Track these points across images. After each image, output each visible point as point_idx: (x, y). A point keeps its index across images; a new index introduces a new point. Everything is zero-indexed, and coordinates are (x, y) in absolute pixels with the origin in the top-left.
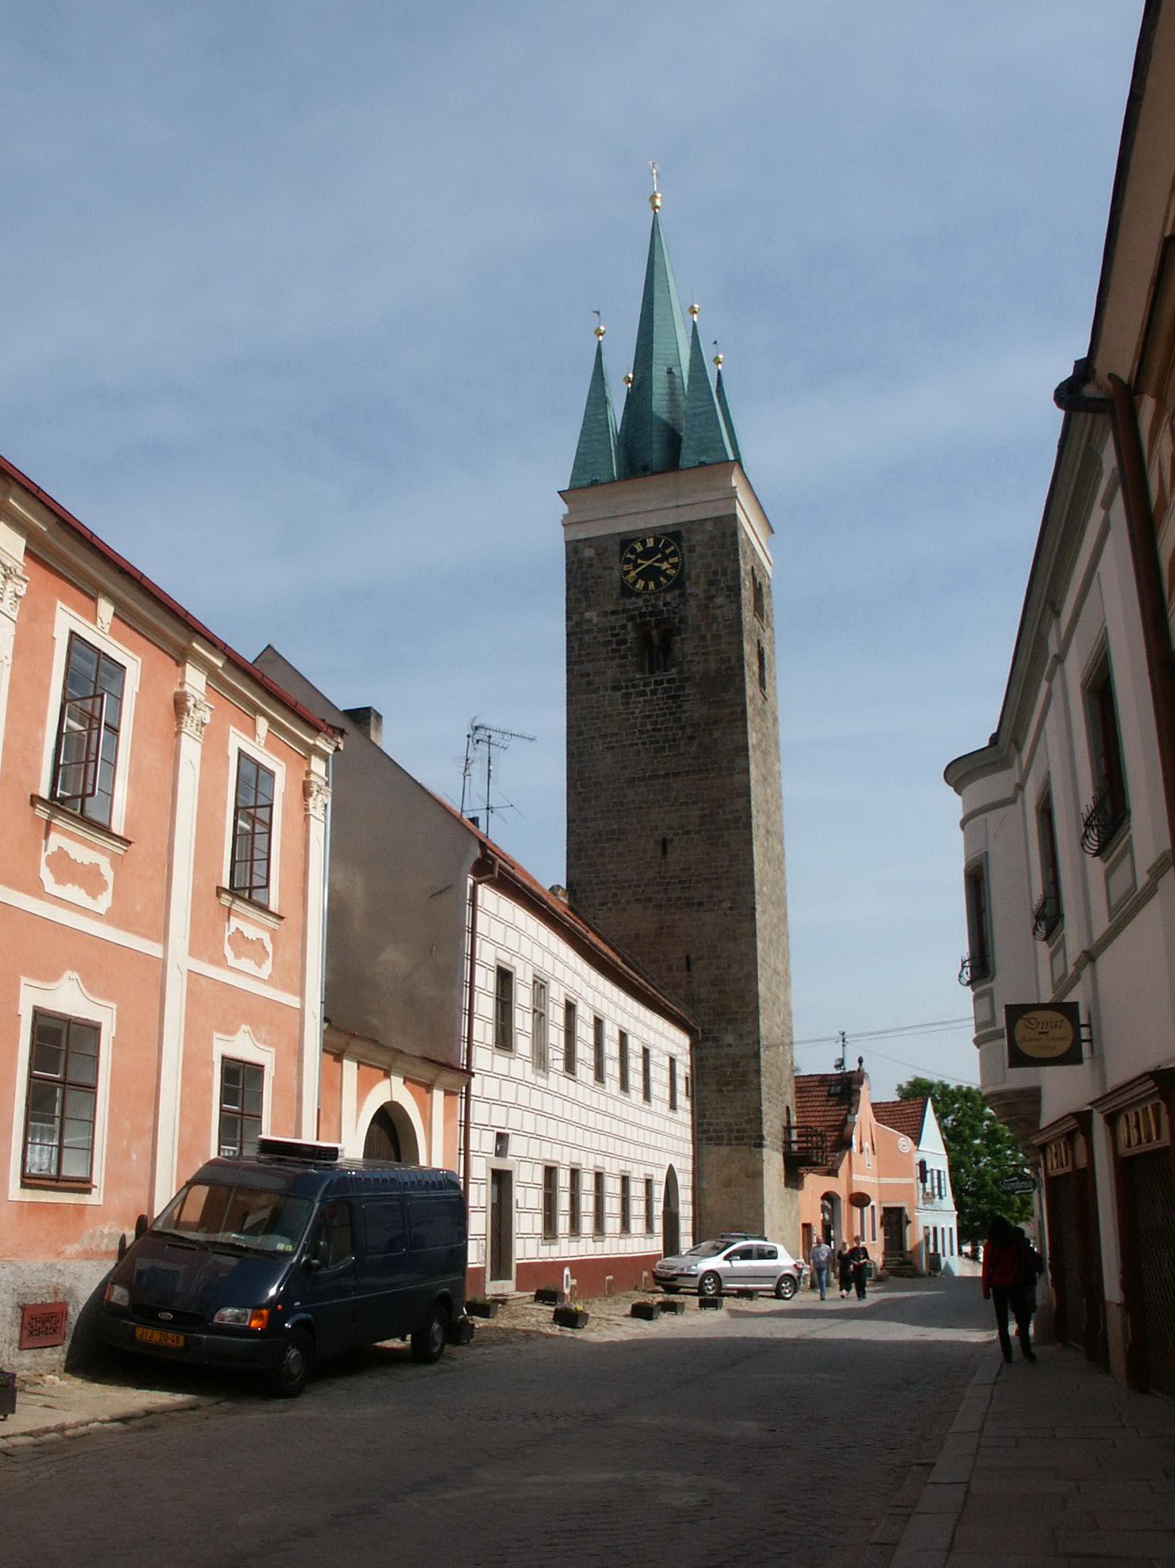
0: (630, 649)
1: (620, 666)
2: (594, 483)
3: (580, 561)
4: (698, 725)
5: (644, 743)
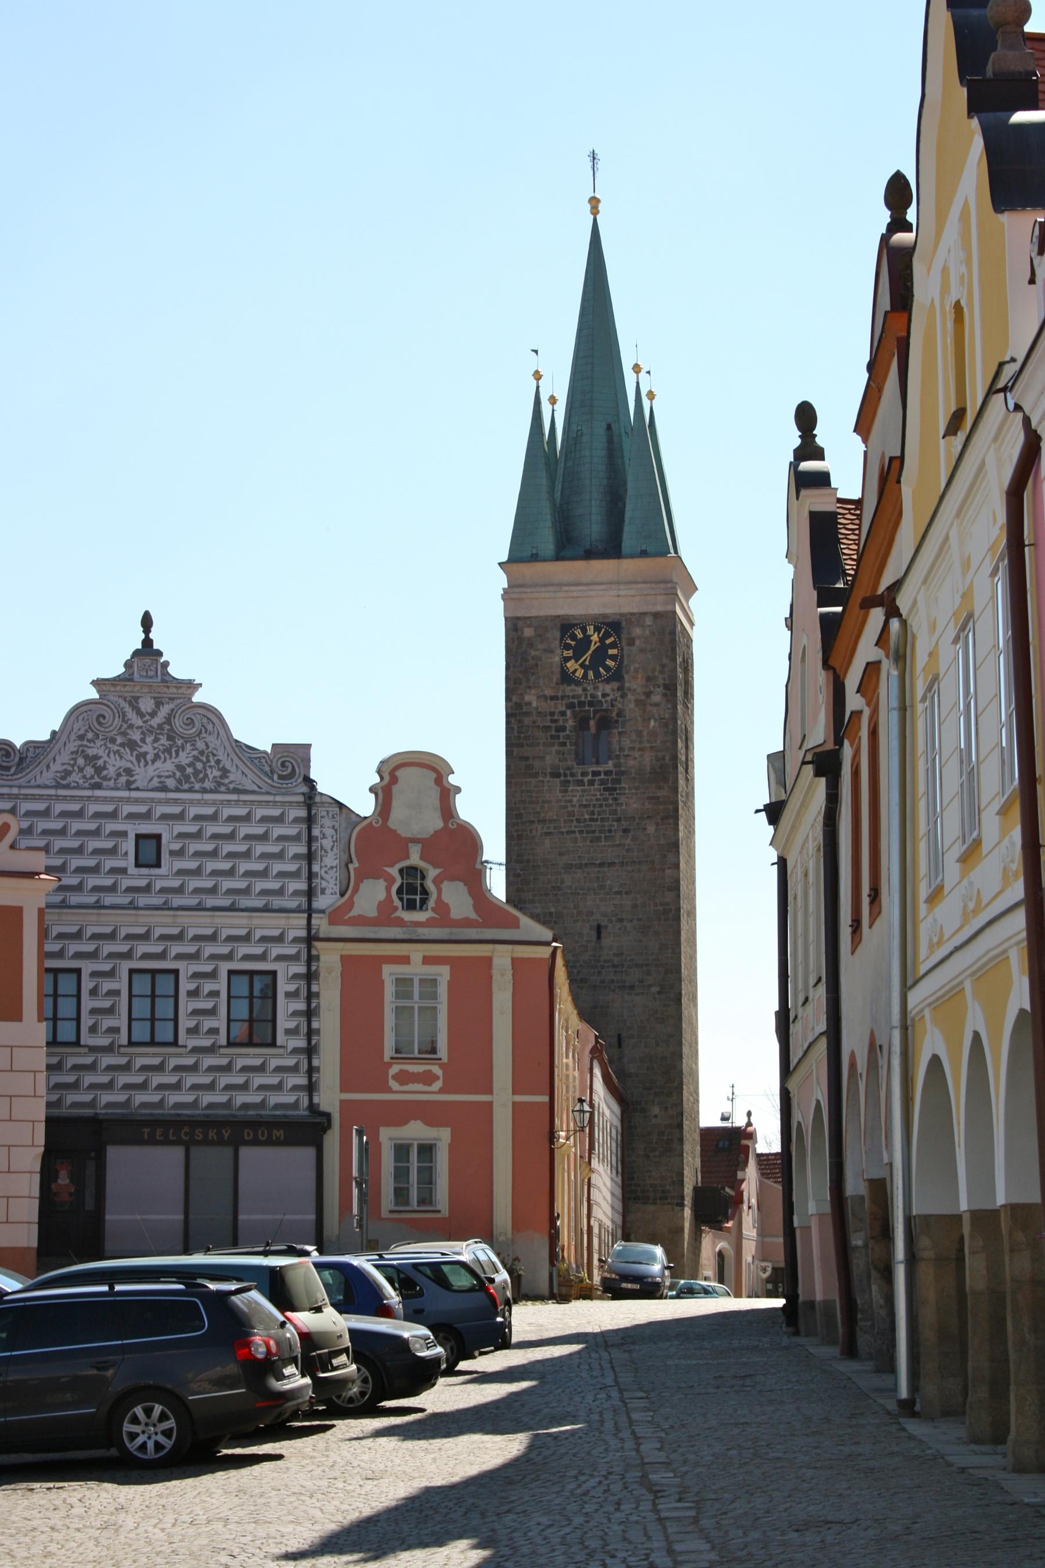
0: (568, 737)
1: (558, 752)
2: (535, 558)
3: (521, 639)
4: (633, 818)
5: (581, 832)
